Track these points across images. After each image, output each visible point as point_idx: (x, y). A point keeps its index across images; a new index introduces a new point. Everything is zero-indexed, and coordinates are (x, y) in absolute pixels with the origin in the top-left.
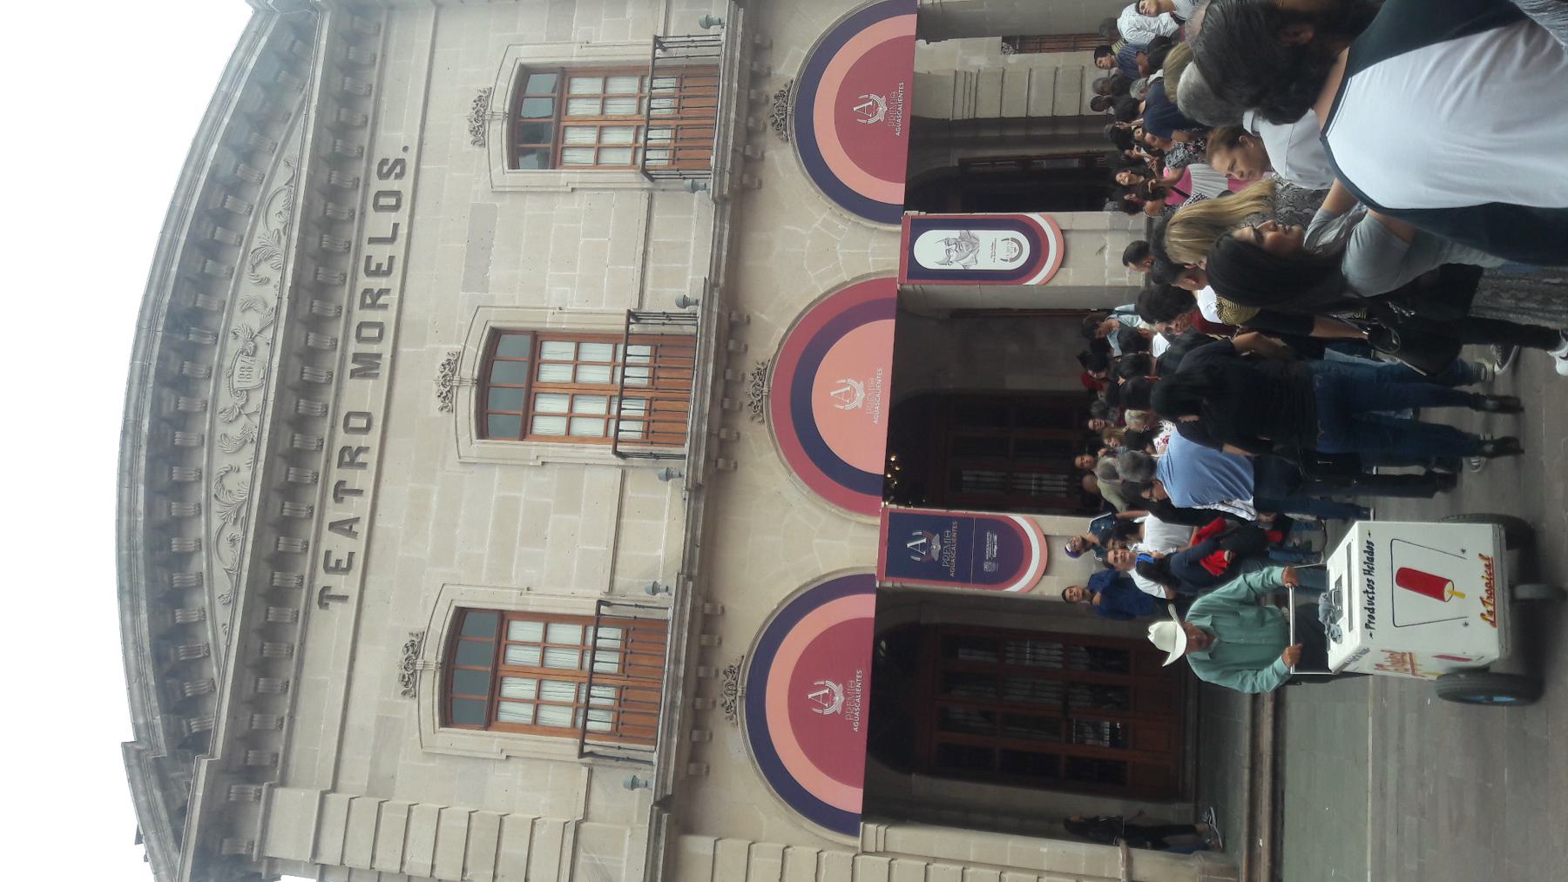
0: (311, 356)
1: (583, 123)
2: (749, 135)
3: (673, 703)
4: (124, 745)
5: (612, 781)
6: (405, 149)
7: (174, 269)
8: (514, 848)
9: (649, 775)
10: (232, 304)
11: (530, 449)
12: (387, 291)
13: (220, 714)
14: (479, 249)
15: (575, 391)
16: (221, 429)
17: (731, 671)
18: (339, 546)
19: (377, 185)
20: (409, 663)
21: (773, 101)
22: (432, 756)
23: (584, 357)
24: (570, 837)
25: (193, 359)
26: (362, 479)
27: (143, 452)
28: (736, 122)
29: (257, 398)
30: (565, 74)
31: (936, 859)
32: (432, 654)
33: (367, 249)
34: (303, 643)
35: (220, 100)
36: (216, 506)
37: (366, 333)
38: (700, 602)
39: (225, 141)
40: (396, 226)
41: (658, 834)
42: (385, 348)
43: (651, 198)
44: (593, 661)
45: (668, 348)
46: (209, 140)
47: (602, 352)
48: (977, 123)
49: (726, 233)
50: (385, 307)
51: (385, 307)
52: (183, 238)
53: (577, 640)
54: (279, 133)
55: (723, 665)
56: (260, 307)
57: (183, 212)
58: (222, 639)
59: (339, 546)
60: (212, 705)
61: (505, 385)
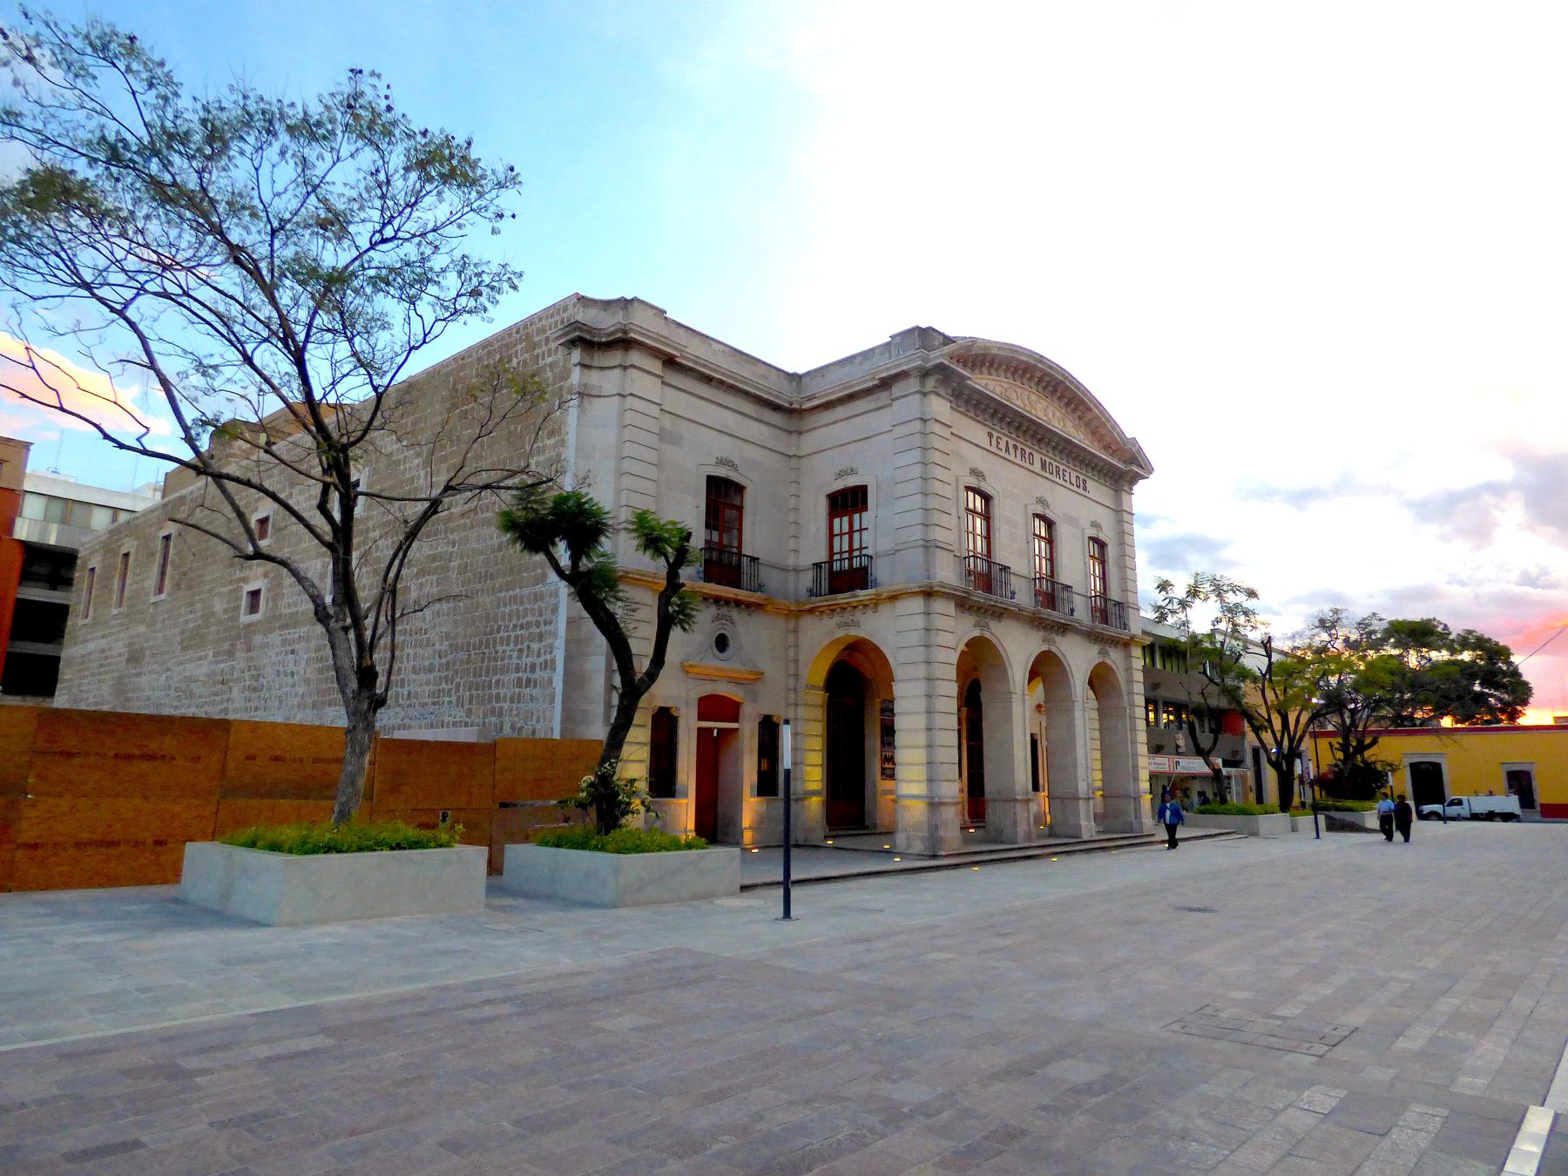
35: (1109, 419)
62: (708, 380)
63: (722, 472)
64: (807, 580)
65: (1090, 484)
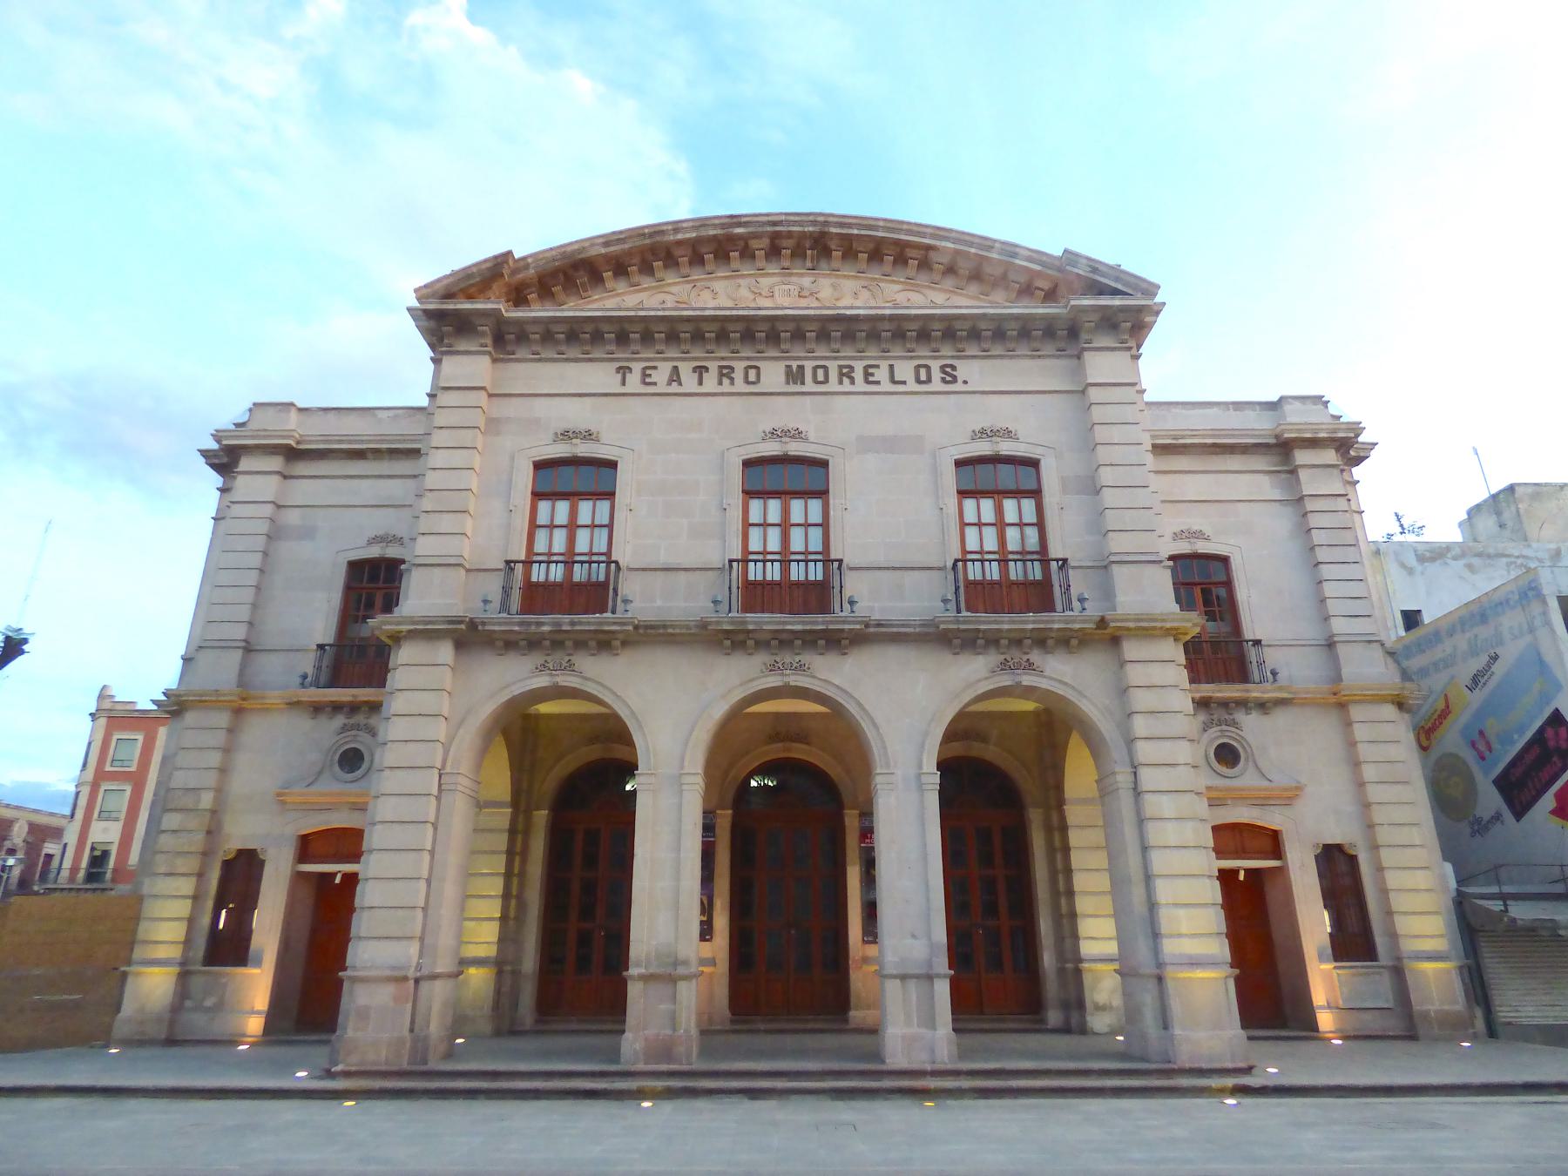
0: (799, 336)
1: (999, 511)
3: (542, 624)
4: (510, 253)
5: (492, 587)
6: (965, 382)
7: (856, 232)
8: (446, 523)
9: (493, 612)
10: (837, 277)
11: (737, 498)
12: (853, 382)
13: (539, 311)
14: (889, 444)
15: (785, 526)
18: (661, 375)
19: (935, 366)
20: (576, 434)
21: (1025, 658)
22: (512, 458)
23: (811, 529)
24: (452, 561)
25: (793, 255)
26: (710, 383)
27: (719, 232)
30: (1036, 494)
31: (435, 829)
32: (583, 449)
33: (884, 365)
34: (590, 360)
35: (987, 243)
36: (689, 286)
37: (820, 372)
38: (621, 636)
39: (957, 252)
40: (904, 383)
42: (809, 386)
43: (939, 569)
44: (582, 562)
45: (818, 596)
46: (955, 241)
47: (816, 544)
48: (1064, 828)
50: (841, 382)
51: (841, 382)
52: (880, 234)
53: (555, 550)
54: (973, 288)
57: (899, 231)
58: (594, 306)
59: (661, 375)
60: (548, 305)
62: (359, 455)
63: (374, 552)
64: (307, 664)
65: (964, 369)
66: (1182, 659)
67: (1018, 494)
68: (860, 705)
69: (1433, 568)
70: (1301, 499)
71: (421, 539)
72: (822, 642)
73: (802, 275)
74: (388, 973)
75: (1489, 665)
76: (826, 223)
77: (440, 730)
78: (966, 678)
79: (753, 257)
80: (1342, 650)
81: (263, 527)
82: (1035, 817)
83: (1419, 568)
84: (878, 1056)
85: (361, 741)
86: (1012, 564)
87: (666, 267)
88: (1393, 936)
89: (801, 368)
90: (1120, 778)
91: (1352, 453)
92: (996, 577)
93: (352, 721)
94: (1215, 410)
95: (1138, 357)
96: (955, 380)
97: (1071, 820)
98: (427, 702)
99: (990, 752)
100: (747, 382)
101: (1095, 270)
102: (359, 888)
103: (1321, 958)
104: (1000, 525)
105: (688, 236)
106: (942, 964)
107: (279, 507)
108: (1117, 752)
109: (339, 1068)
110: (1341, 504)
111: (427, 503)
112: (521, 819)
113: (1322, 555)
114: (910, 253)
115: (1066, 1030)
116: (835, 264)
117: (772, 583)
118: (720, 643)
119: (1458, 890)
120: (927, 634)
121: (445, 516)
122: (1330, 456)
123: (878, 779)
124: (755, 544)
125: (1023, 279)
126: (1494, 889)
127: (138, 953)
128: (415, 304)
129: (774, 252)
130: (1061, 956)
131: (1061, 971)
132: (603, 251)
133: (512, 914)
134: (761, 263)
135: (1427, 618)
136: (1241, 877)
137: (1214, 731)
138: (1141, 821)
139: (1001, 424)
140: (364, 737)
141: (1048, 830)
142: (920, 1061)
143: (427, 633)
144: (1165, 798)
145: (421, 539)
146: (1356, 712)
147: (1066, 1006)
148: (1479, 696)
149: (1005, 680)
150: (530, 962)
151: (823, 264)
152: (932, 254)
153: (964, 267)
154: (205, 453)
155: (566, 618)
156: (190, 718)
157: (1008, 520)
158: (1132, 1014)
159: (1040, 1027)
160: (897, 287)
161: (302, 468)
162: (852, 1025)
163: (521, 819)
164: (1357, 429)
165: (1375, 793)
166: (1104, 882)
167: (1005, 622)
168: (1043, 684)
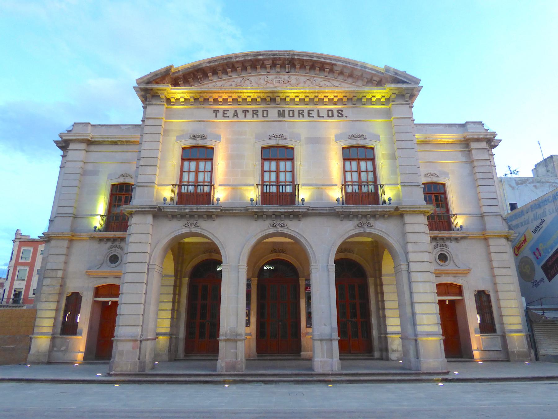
1: (359, 166)
2: (355, 215)
3: (186, 209)
6: (346, 117)
7: (305, 58)
10: (298, 75)
12: (303, 116)
15: (278, 172)
16: (262, 77)
17: (197, 225)
21: (368, 222)
25: (281, 67)
27: (253, 58)
28: (359, 212)
29: (271, 86)
30: (373, 160)
31: (147, 285)
35: (355, 64)
37: (291, 112)
38: (216, 213)
39: (344, 66)
41: (151, 208)
44: (201, 185)
47: (289, 178)
48: (381, 285)
49: (325, 211)
50: (299, 117)
52: (314, 59)
53: (191, 180)
54: (350, 80)
55: (199, 222)
56: (297, 83)
59: (230, 114)
61: (278, 153)
62: (115, 143)
63: (121, 180)
66: (426, 222)
67: (366, 159)
68: (306, 240)
69: (522, 187)
70: (472, 161)
71: (139, 176)
72: (291, 216)
73: (284, 75)
74: (130, 338)
75: (541, 224)
76: (294, 55)
77: (148, 249)
78: (346, 229)
79: (266, 67)
80: (486, 218)
81: (79, 171)
82: (371, 281)
83: (517, 187)
84: (311, 369)
85: (118, 252)
86: (363, 186)
87: (232, 71)
88: (502, 324)
89: (284, 111)
90: (402, 267)
91: (492, 144)
92: (357, 191)
93: (114, 244)
94: (441, 127)
95: (412, 107)
96: (342, 115)
97: (384, 282)
98: (143, 238)
99: (354, 257)
100: (263, 116)
101: (396, 74)
102: (116, 328)
103: (476, 332)
104: (359, 171)
105: (240, 59)
106: (335, 335)
107: (85, 163)
108: (402, 257)
109: (113, 372)
110: (488, 163)
111: (142, 163)
112: (178, 280)
113: (482, 195)
114: (326, 66)
115: (381, 359)
116: (297, 71)
117: (273, 193)
118: (253, 216)
119: (527, 308)
120: (331, 213)
121: (149, 167)
122: (484, 145)
123: (312, 267)
124: (266, 178)
125: (369, 77)
126: (540, 307)
127: (36, 330)
128: (136, 85)
129: (274, 66)
130: (380, 332)
131: (380, 338)
132: (208, 65)
133: (175, 317)
134: (269, 70)
135: (519, 206)
136: (447, 303)
137: (438, 249)
138: (410, 283)
139: (359, 133)
140: (118, 250)
141: (376, 286)
142: (327, 370)
143: (142, 212)
144: (419, 274)
145: (139, 176)
146: (491, 242)
147: (381, 350)
148: (537, 235)
149: (360, 230)
150: (182, 334)
151: (293, 70)
152: (334, 67)
153: (347, 72)
154: (56, 142)
155: (195, 206)
156: (53, 243)
157: (362, 170)
158: (405, 353)
159: (372, 358)
160: (322, 79)
161: (93, 148)
162: (302, 357)
163: (178, 280)
164: (494, 134)
165: (497, 272)
166: (396, 305)
167: (361, 209)
168: (375, 232)
